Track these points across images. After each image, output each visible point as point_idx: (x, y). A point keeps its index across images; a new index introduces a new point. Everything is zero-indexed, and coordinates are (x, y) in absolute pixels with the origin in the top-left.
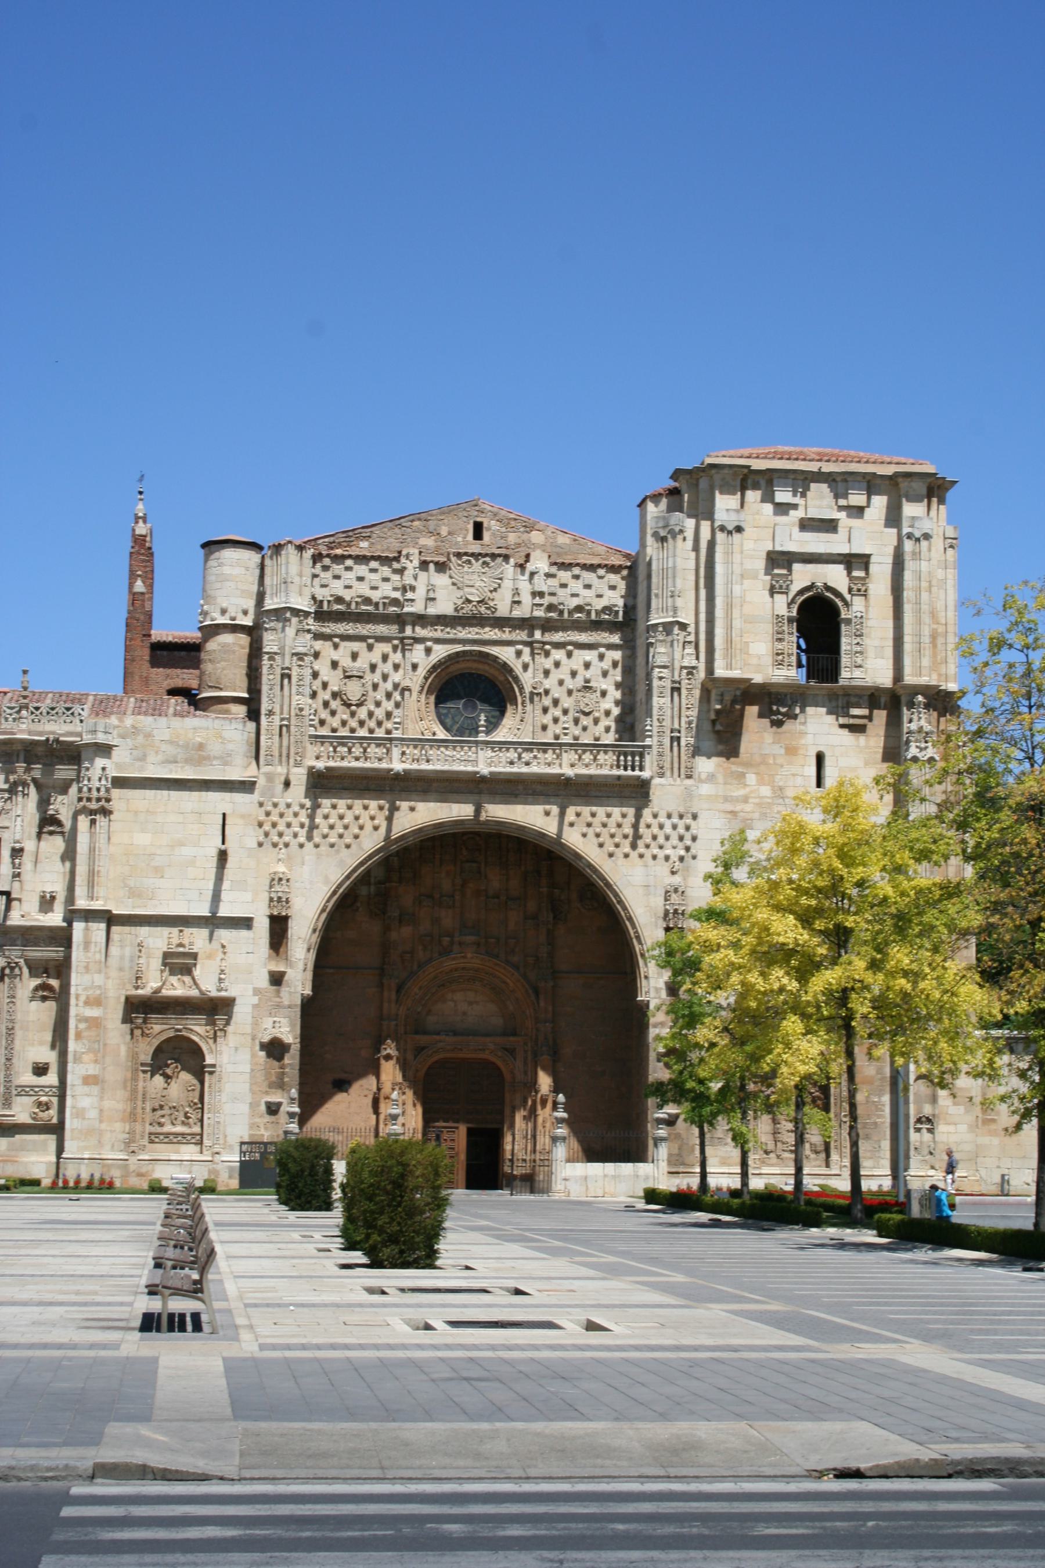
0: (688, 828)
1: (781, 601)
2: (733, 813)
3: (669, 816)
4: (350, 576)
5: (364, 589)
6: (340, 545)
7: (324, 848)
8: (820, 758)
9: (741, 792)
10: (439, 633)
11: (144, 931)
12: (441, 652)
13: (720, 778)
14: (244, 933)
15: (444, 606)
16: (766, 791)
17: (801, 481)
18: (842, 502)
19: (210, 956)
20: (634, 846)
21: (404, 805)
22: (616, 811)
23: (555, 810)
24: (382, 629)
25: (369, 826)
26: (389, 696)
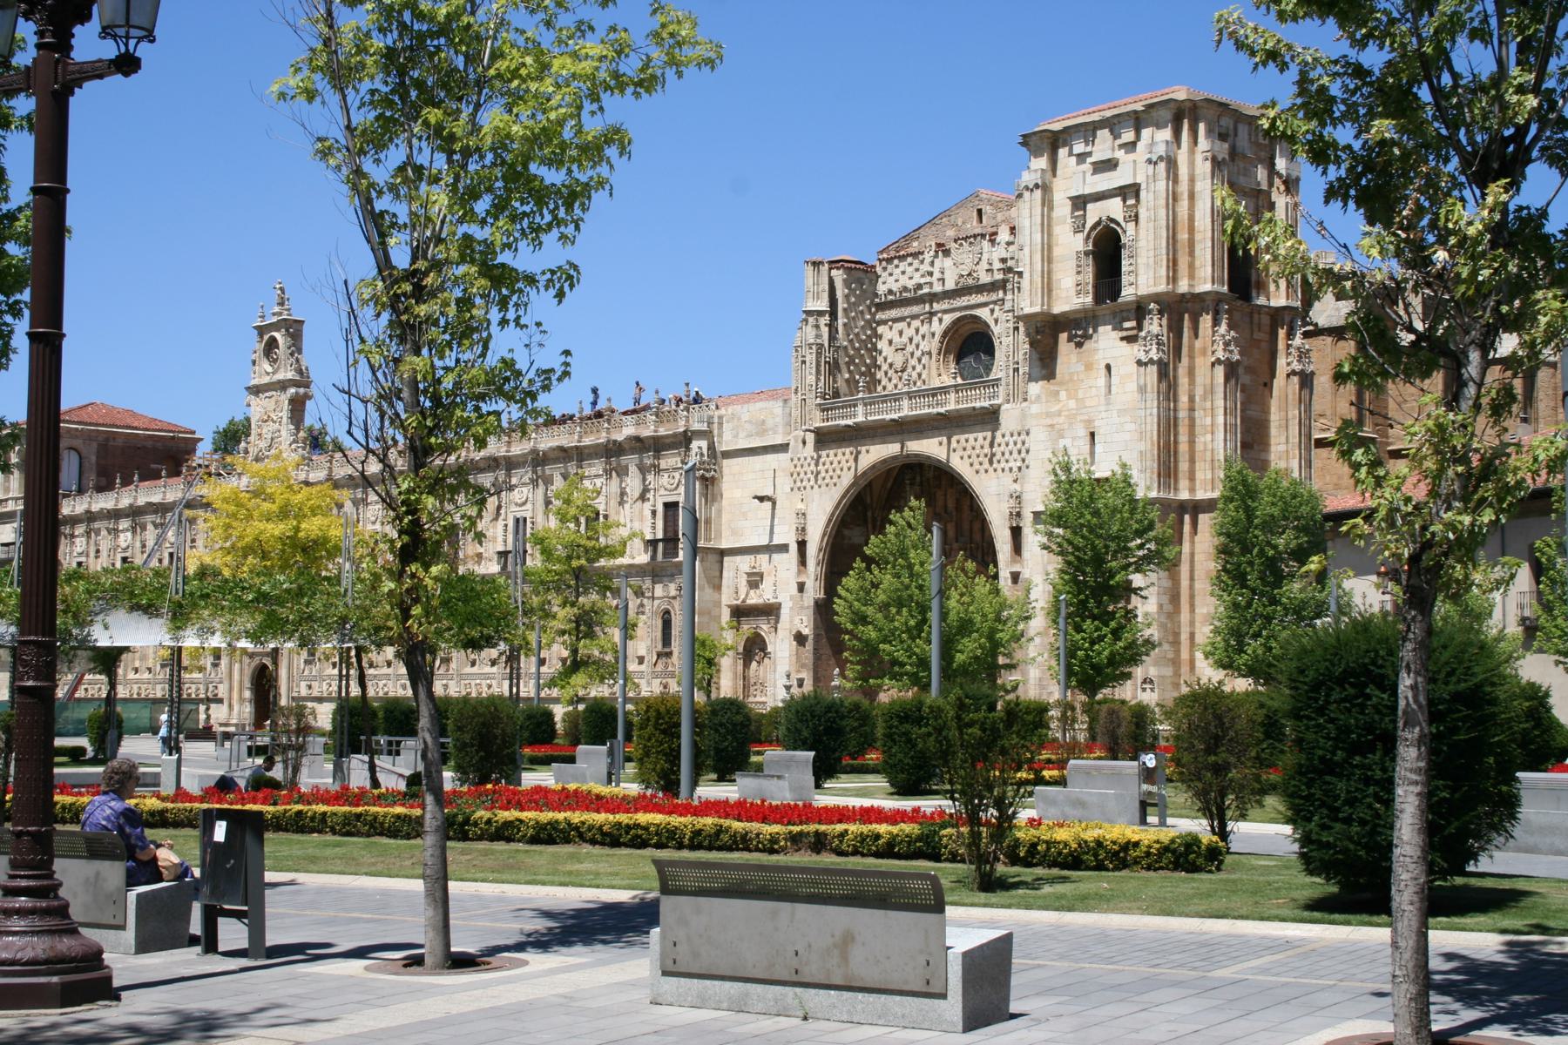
0: (1023, 443)
1: (1081, 237)
2: (1052, 426)
3: (1012, 435)
4: (898, 271)
5: (904, 281)
6: (902, 247)
7: (823, 487)
8: (1108, 367)
9: (1055, 408)
10: (945, 305)
11: (738, 558)
12: (948, 319)
13: (1043, 396)
14: (785, 555)
15: (950, 285)
16: (1072, 404)
17: (1088, 131)
18: (1119, 142)
19: (769, 574)
20: (991, 462)
21: (863, 449)
22: (980, 435)
23: (945, 439)
24: (915, 309)
25: (845, 469)
26: (920, 360)
